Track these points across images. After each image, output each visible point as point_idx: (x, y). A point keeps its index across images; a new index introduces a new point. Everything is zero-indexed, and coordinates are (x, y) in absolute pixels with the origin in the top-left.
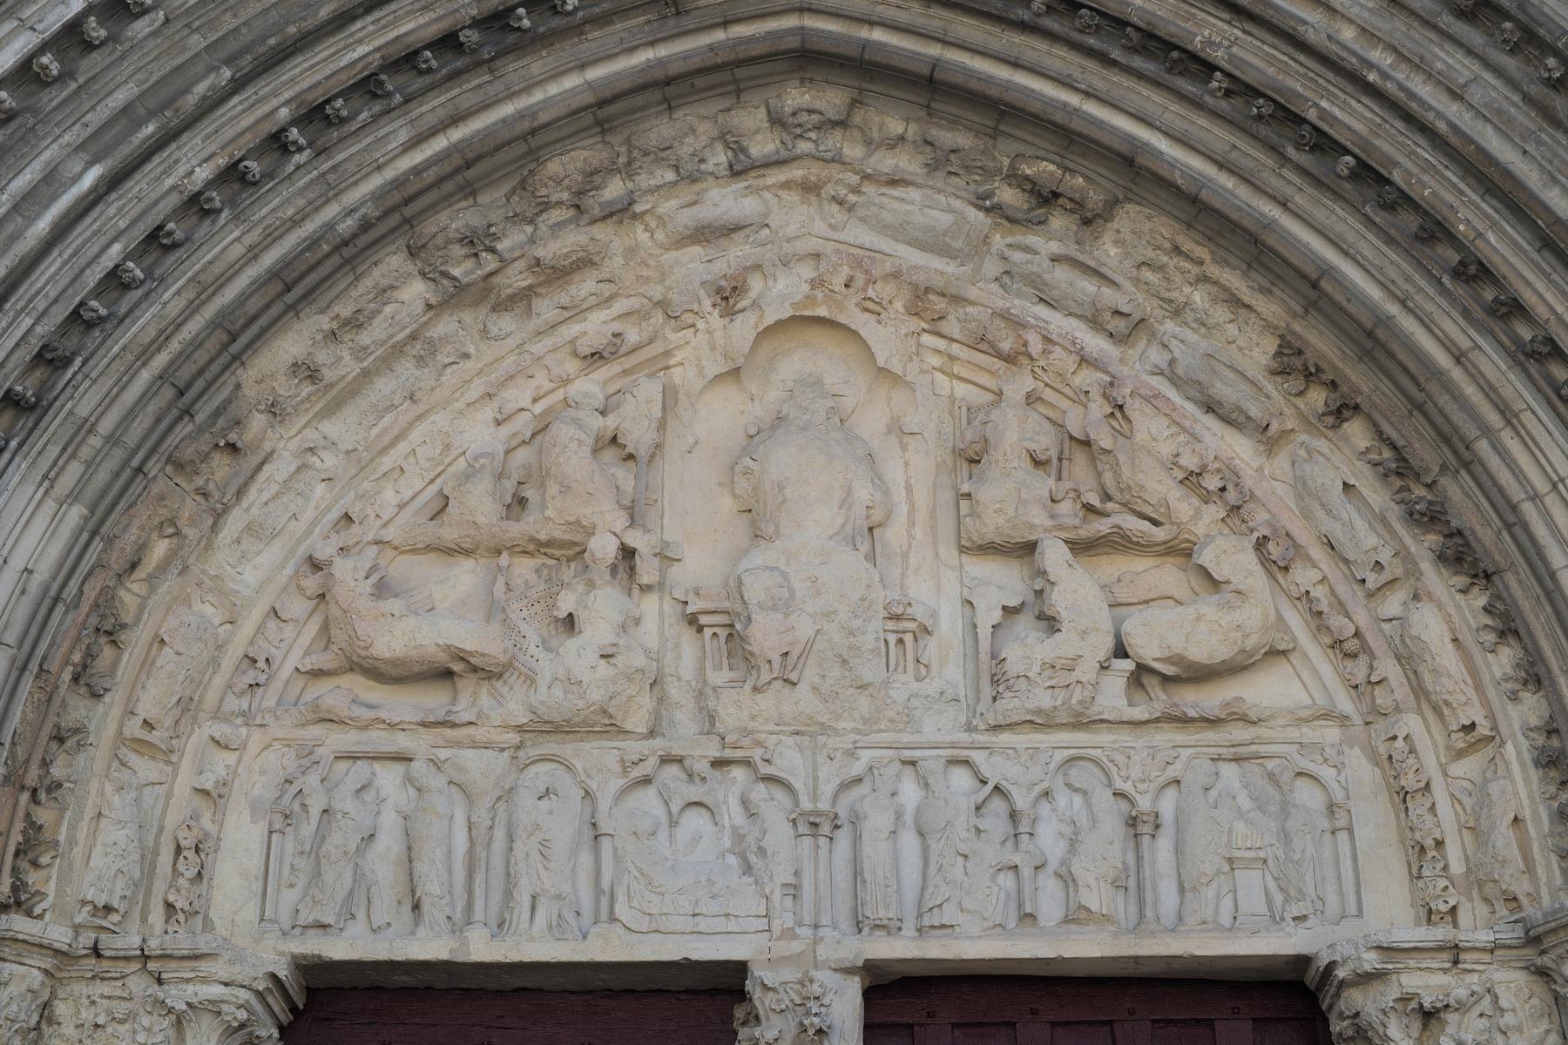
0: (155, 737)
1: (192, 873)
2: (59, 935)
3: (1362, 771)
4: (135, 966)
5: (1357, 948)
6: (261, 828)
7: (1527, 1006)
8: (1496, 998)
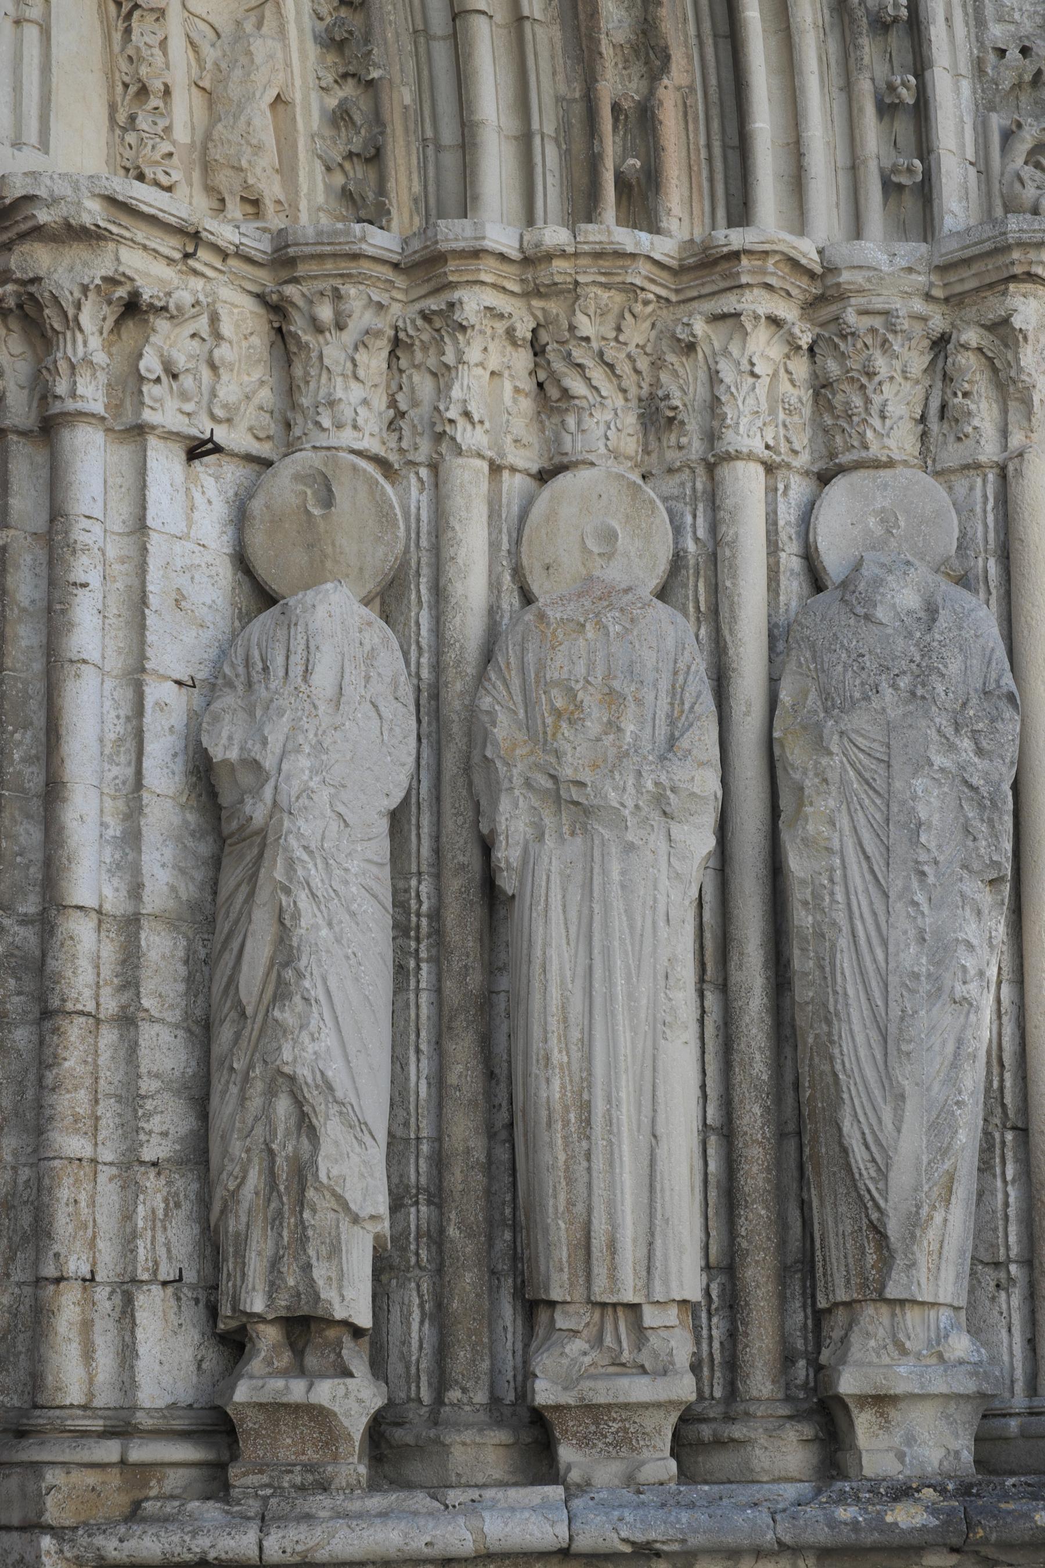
5: (76, 189)
7: (244, 344)
8: (214, 319)
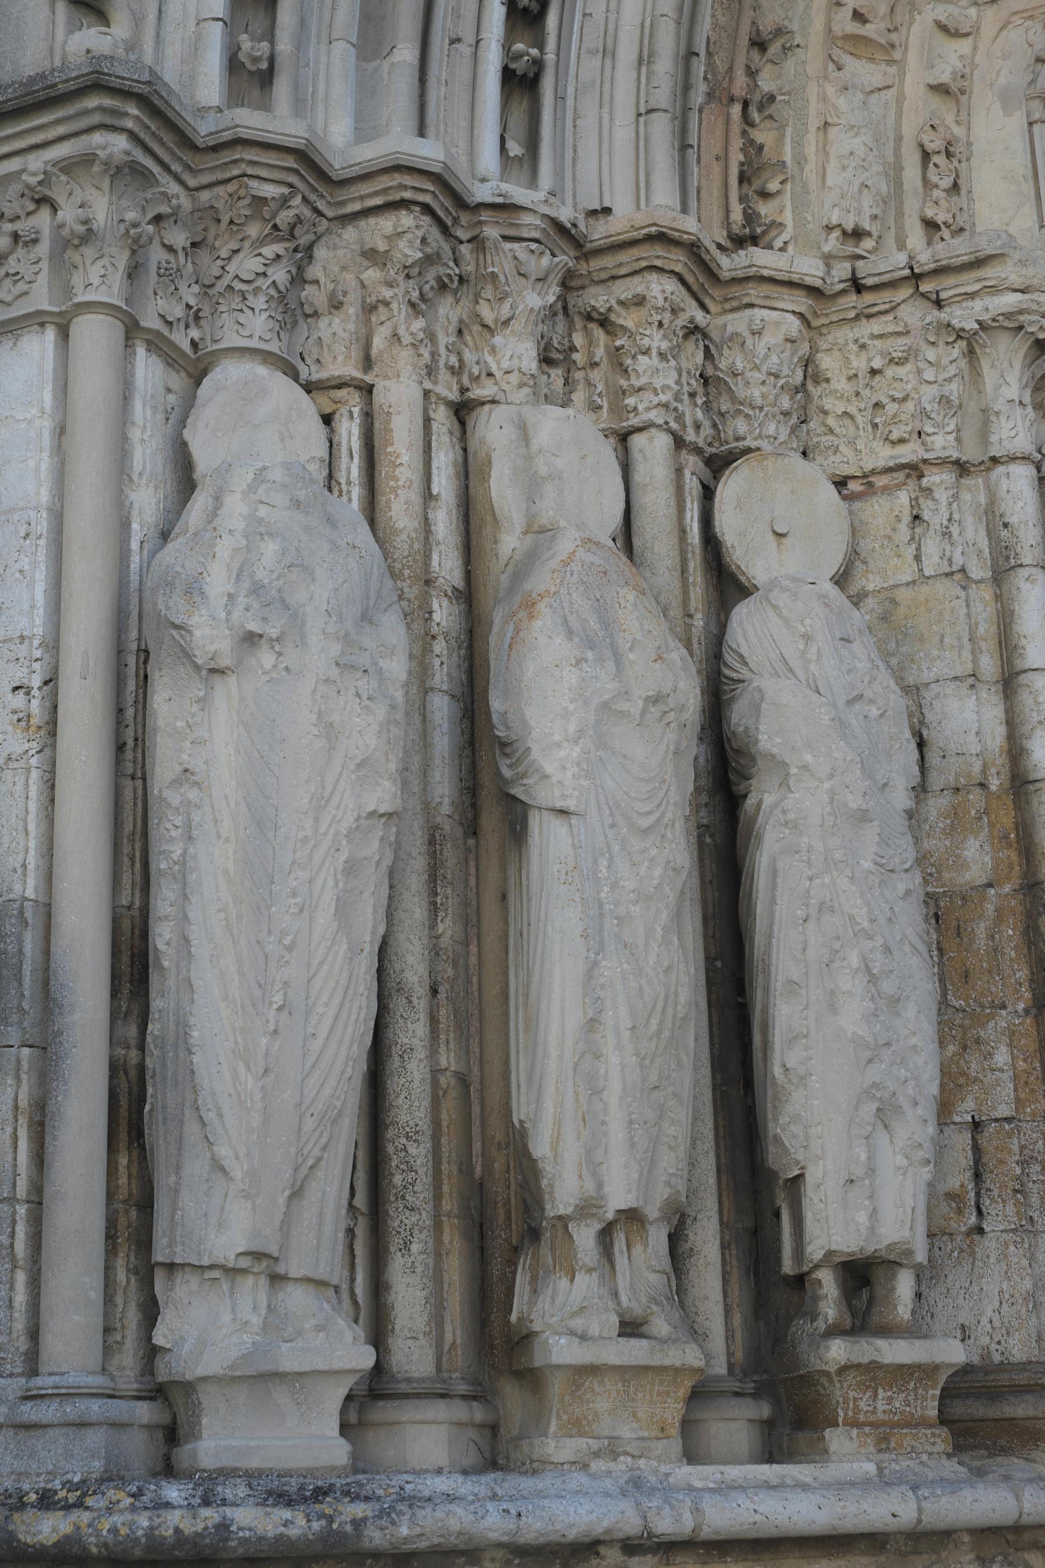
0: (869, 30)
1: (947, 182)
2: (808, 268)
4: (904, 292)
6: (1017, 122)
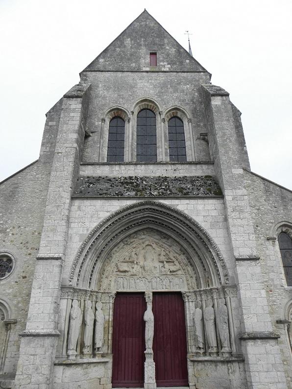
3: (185, 278)
